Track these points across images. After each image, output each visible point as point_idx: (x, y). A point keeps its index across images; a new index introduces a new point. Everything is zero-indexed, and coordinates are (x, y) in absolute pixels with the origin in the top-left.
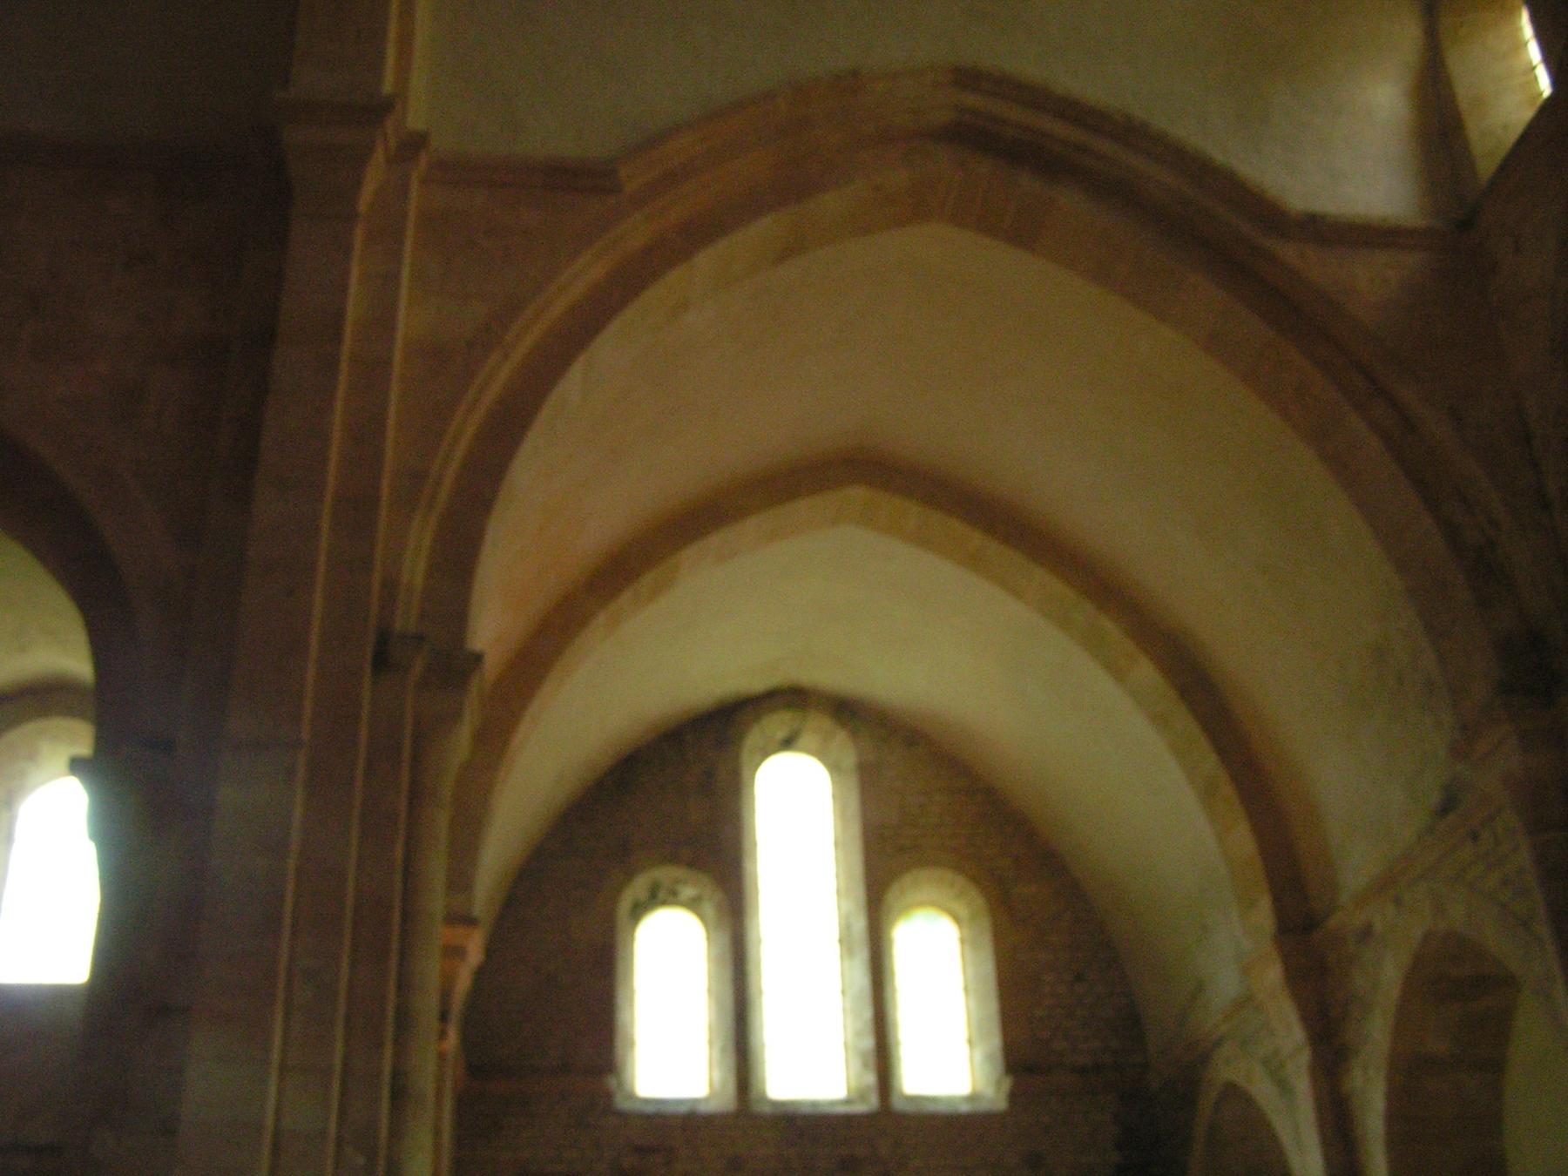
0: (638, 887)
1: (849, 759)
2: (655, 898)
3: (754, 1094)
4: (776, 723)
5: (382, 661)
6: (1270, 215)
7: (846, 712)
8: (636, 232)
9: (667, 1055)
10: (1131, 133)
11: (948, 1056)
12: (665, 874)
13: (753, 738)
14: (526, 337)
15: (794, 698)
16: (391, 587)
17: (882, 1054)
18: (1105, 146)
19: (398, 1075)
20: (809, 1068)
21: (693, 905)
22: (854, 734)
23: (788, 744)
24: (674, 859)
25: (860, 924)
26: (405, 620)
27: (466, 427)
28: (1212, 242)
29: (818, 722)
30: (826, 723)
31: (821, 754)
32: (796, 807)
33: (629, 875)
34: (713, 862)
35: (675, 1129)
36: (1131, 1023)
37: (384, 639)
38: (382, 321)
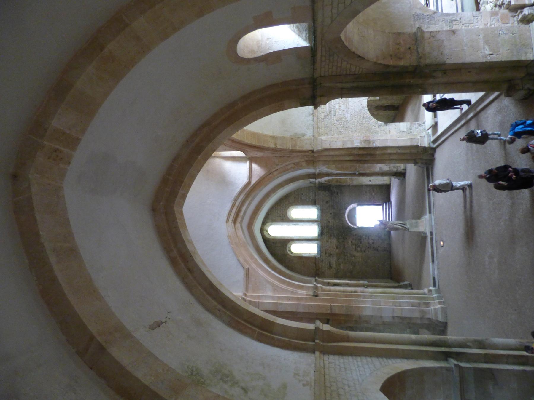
0: (289, 253)
1: (271, 223)
2: (290, 251)
3: (316, 238)
4: (265, 233)
5: (317, 296)
6: (249, 183)
7: (264, 223)
8: (254, 266)
9: (311, 249)
10: (236, 200)
11: (311, 212)
12: (287, 249)
13: (267, 236)
14: (271, 280)
15: (262, 230)
16: (307, 295)
17: (313, 221)
18: (237, 204)
19: (361, 292)
20: (313, 231)
21: (291, 245)
22: (267, 222)
23: (267, 231)
24: (286, 248)
25: (295, 223)
26: (311, 293)
27: (285, 287)
29: (265, 227)
30: (265, 226)
31: (269, 226)
32: (276, 230)
33: (288, 254)
34: (286, 242)
35: (321, 249)
37: (314, 295)
38: (272, 297)
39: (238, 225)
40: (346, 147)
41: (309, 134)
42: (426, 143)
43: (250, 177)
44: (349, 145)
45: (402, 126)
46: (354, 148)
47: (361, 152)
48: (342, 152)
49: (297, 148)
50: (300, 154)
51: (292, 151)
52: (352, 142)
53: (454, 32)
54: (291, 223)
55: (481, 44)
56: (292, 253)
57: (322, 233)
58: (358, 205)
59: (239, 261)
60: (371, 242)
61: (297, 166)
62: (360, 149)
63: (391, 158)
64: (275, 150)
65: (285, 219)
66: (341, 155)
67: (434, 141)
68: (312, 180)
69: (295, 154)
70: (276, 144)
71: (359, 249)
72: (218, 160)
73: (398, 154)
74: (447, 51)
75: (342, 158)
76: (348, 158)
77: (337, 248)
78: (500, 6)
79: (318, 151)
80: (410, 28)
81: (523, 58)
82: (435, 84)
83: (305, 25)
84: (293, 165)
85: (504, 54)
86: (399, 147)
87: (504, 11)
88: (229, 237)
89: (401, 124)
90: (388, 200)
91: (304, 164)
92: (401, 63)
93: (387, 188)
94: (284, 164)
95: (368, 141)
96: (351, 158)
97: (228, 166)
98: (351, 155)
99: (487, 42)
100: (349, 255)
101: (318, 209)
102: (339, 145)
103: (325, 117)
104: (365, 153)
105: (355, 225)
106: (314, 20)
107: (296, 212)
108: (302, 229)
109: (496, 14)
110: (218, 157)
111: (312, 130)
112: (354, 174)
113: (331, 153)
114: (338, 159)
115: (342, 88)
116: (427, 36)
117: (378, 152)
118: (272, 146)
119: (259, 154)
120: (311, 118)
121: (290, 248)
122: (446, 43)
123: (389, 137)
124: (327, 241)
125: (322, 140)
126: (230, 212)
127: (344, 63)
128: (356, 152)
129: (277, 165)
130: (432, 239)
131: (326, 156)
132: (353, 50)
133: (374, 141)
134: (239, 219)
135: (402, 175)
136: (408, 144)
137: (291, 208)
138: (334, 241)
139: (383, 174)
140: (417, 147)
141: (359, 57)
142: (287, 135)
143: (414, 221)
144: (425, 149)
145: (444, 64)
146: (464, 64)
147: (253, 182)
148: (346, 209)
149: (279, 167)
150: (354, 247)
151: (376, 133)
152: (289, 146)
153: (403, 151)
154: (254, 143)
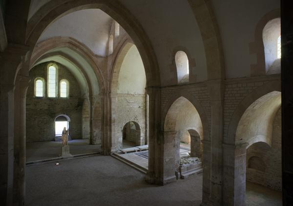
1: (58, 68)
2: (38, 79)
4: (51, 64)
6: (93, 54)
7: (58, 64)
8: (39, 51)
9: (39, 92)
10: (84, 45)
11: (64, 94)
15: (53, 62)
20: (52, 94)
28: (88, 55)
29: (55, 65)
32: (52, 71)
34: (45, 77)
36: (80, 92)
39: (68, 45)
40: (112, 110)
41: (119, 92)
42: (113, 150)
43: (97, 56)
44: (112, 112)
45: (121, 139)
46: (111, 115)
47: (108, 118)
48: (109, 109)
49: (112, 84)
50: (108, 86)
51: (110, 81)
52: (114, 114)
53: (174, 146)
54: (57, 81)
55: (169, 158)
56: (36, 80)
57: (51, 99)
58: (70, 122)
59: (43, 41)
60: (45, 130)
61: (100, 84)
62: (111, 118)
63: (105, 134)
64: (112, 72)
65: (60, 77)
66: (107, 108)
67: (113, 154)
68: (87, 95)
69: (109, 83)
70: (115, 72)
71: (40, 122)
72: (107, 38)
73: (107, 138)
74: (168, 144)
75: (105, 108)
76: (105, 112)
77: (41, 109)
78: (180, 164)
79: (110, 96)
80: (177, 129)
81: (164, 174)
82: (154, 142)
83: (188, 81)
84: (102, 81)
85: (166, 167)
86: (111, 138)
87: (179, 165)
88: (60, 37)
89: (122, 138)
90: (73, 139)
91: (103, 88)
92: (165, 125)
93: (80, 138)
94: (103, 76)
95: (114, 122)
96: (105, 114)
97: (104, 44)
98: (107, 112)
99: (170, 159)
100: (35, 116)
101: (66, 98)
102: (113, 107)
103: (126, 100)
104: (108, 121)
105: (56, 121)
106: (190, 84)
107: (64, 85)
108: (52, 86)
109: (178, 163)
110: (109, 39)
111: (121, 93)
112: (91, 117)
113: (108, 103)
114: (105, 106)
115: (154, 101)
116: (174, 135)
117: (108, 127)
118: (115, 70)
119: (110, 63)
120: (126, 93)
121: (40, 79)
122: (171, 144)
123: (116, 132)
124: (45, 103)
125: (115, 98)
126: (76, 41)
127: (167, 100)
128: (109, 116)
129: (103, 72)
130: (59, 159)
131: (107, 100)
132: (174, 103)
133: (114, 125)
134: (71, 46)
135: (91, 143)
136: (112, 142)
137: (68, 82)
138: (46, 108)
139: (91, 133)
140: (111, 146)
141: (170, 106)
142: (119, 79)
143: (69, 149)
144: (109, 150)
145: (163, 143)
146: (163, 151)
147: (94, 58)
148: (67, 115)
149: (102, 74)
150: (42, 120)
151: (118, 126)
152: (114, 80)
153: (108, 140)
154: (118, 60)
